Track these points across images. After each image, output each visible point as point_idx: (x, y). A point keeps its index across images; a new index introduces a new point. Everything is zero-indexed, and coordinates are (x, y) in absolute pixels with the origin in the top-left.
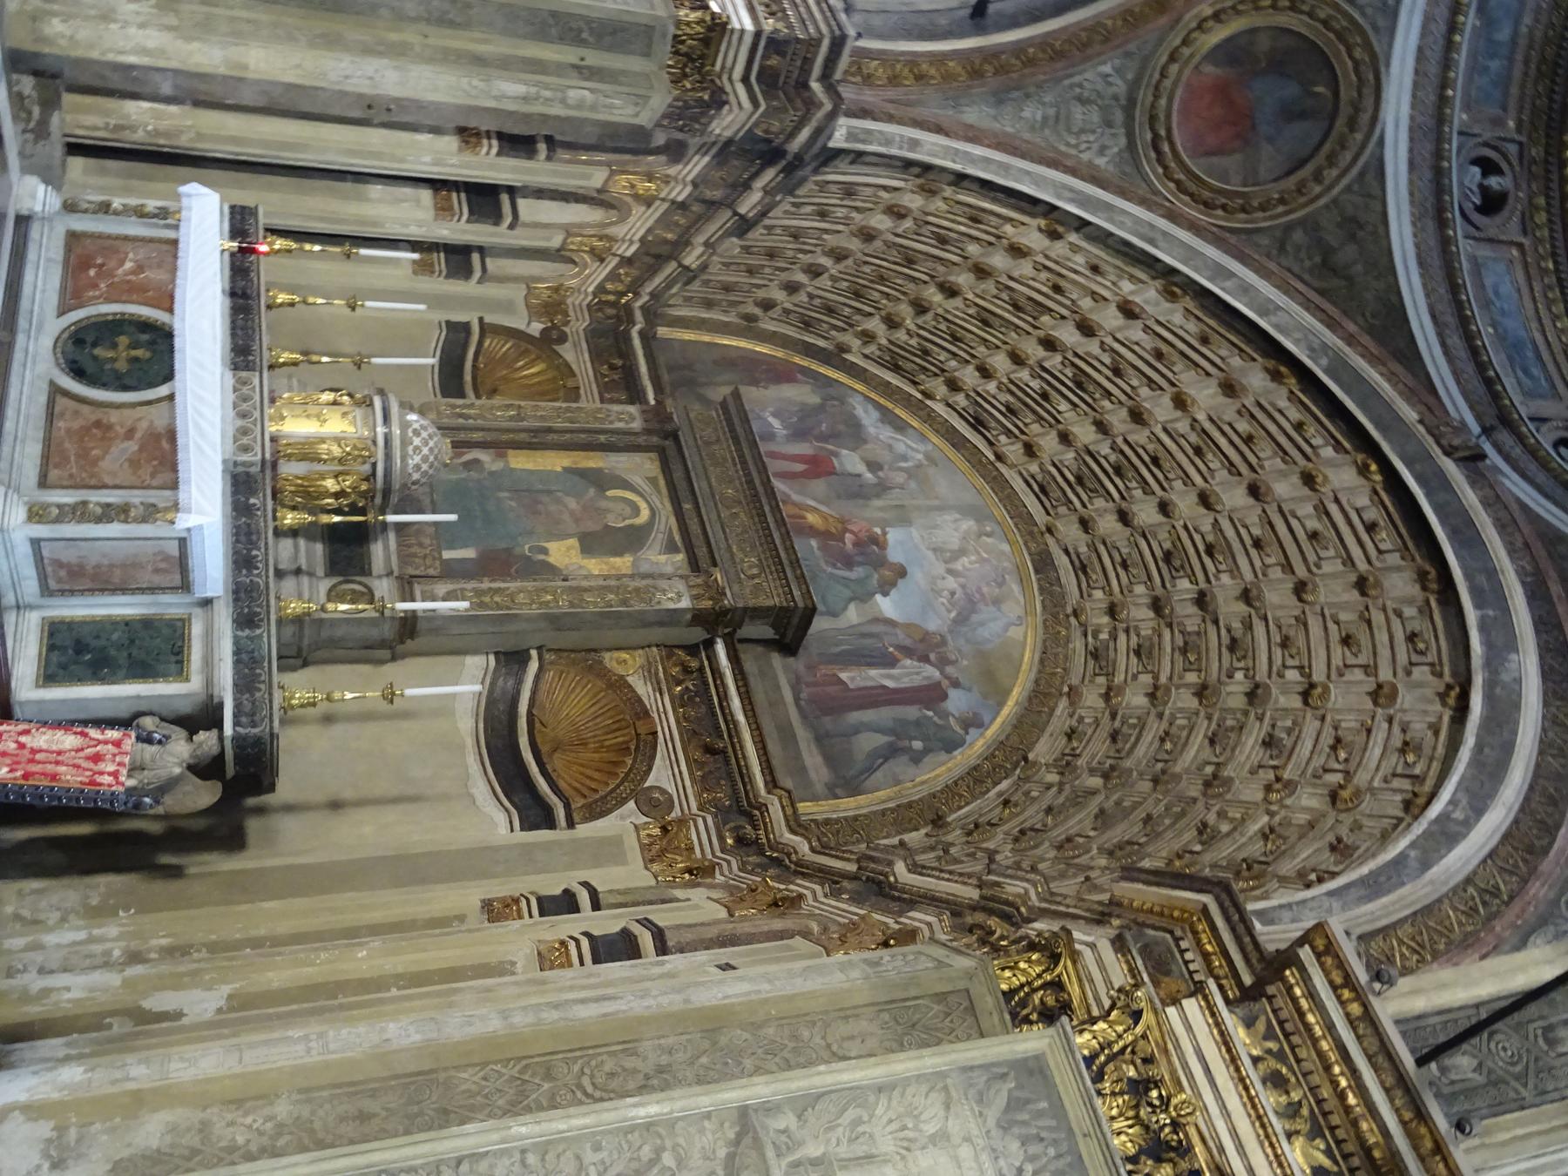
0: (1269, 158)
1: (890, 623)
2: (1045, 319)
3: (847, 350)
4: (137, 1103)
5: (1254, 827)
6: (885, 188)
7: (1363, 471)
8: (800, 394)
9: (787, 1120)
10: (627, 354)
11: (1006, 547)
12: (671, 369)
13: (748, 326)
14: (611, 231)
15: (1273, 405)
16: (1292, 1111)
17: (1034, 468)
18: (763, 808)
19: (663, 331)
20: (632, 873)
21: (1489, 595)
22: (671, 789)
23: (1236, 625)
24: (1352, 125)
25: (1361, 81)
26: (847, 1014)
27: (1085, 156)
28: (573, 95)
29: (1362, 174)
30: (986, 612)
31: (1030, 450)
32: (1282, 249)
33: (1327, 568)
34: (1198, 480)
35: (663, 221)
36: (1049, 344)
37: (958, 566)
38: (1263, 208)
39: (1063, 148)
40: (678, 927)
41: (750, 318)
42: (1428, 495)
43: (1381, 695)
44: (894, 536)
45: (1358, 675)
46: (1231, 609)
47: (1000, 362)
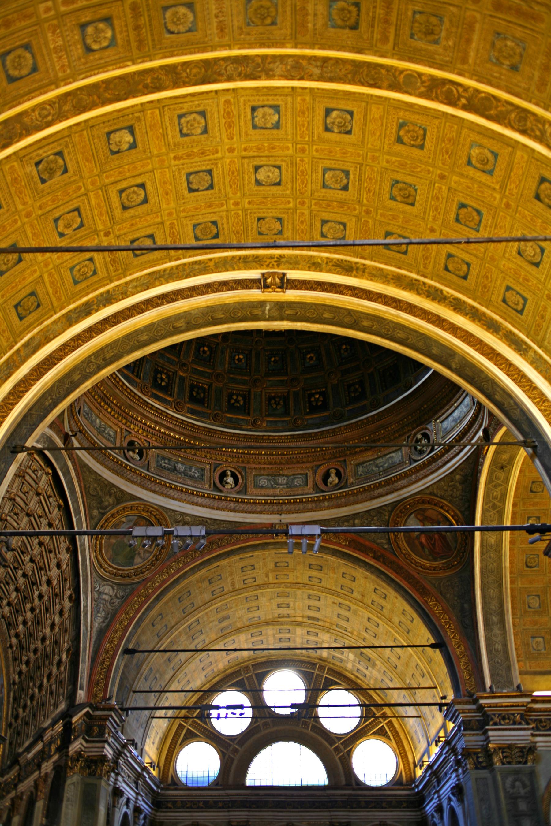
43: (59, 566)
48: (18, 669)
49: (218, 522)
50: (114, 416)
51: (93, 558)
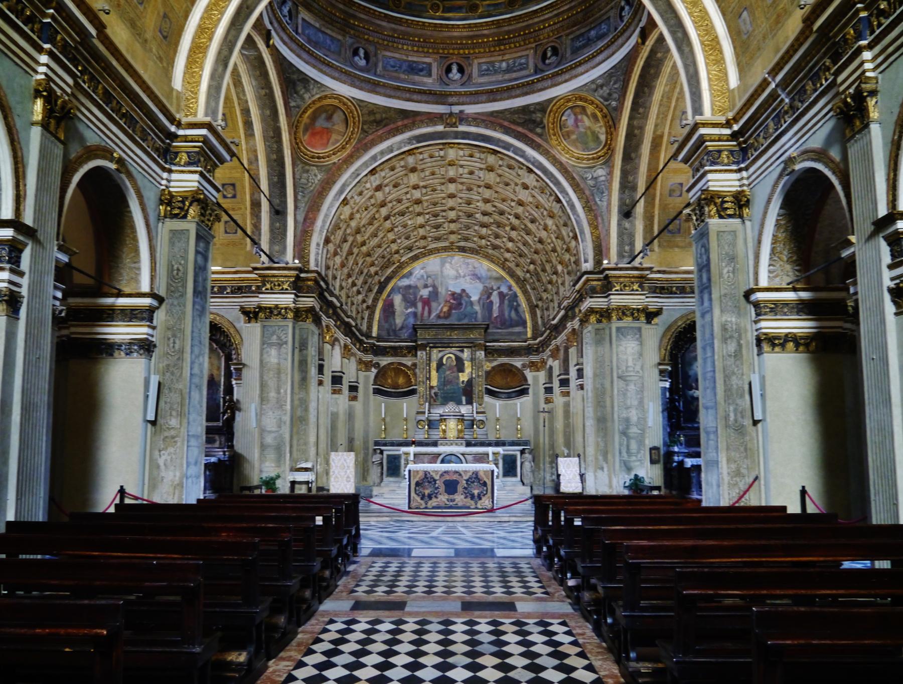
0: (340, 127)
1: (480, 299)
2: (377, 216)
3: (380, 280)
4: (596, 459)
5: (554, 239)
6: (327, 254)
7: (452, 148)
8: (398, 300)
9: (620, 371)
10: (385, 348)
11: (456, 258)
12: (389, 336)
13: (372, 309)
14: (342, 345)
15: (421, 160)
16: (629, 286)
17: (430, 239)
18: (529, 345)
19: (374, 334)
20: (542, 375)
21: (508, 146)
22: (522, 363)
23: (494, 209)
24: (344, 104)
25: (335, 98)
26: (596, 352)
27: (316, 182)
28: (313, 353)
29: (359, 106)
30: (477, 272)
31: (424, 238)
32: (366, 132)
33: (481, 175)
34: (443, 195)
35: (338, 328)
36: (387, 218)
37: (462, 274)
38: (352, 134)
39: (312, 188)
40: (560, 370)
41: (368, 307)
42: (469, 139)
43: (526, 187)
45: (518, 189)
46: (489, 208)
47: (391, 236)
48: (525, 270)
49: (618, 66)
50: (520, 46)
51: (563, 159)
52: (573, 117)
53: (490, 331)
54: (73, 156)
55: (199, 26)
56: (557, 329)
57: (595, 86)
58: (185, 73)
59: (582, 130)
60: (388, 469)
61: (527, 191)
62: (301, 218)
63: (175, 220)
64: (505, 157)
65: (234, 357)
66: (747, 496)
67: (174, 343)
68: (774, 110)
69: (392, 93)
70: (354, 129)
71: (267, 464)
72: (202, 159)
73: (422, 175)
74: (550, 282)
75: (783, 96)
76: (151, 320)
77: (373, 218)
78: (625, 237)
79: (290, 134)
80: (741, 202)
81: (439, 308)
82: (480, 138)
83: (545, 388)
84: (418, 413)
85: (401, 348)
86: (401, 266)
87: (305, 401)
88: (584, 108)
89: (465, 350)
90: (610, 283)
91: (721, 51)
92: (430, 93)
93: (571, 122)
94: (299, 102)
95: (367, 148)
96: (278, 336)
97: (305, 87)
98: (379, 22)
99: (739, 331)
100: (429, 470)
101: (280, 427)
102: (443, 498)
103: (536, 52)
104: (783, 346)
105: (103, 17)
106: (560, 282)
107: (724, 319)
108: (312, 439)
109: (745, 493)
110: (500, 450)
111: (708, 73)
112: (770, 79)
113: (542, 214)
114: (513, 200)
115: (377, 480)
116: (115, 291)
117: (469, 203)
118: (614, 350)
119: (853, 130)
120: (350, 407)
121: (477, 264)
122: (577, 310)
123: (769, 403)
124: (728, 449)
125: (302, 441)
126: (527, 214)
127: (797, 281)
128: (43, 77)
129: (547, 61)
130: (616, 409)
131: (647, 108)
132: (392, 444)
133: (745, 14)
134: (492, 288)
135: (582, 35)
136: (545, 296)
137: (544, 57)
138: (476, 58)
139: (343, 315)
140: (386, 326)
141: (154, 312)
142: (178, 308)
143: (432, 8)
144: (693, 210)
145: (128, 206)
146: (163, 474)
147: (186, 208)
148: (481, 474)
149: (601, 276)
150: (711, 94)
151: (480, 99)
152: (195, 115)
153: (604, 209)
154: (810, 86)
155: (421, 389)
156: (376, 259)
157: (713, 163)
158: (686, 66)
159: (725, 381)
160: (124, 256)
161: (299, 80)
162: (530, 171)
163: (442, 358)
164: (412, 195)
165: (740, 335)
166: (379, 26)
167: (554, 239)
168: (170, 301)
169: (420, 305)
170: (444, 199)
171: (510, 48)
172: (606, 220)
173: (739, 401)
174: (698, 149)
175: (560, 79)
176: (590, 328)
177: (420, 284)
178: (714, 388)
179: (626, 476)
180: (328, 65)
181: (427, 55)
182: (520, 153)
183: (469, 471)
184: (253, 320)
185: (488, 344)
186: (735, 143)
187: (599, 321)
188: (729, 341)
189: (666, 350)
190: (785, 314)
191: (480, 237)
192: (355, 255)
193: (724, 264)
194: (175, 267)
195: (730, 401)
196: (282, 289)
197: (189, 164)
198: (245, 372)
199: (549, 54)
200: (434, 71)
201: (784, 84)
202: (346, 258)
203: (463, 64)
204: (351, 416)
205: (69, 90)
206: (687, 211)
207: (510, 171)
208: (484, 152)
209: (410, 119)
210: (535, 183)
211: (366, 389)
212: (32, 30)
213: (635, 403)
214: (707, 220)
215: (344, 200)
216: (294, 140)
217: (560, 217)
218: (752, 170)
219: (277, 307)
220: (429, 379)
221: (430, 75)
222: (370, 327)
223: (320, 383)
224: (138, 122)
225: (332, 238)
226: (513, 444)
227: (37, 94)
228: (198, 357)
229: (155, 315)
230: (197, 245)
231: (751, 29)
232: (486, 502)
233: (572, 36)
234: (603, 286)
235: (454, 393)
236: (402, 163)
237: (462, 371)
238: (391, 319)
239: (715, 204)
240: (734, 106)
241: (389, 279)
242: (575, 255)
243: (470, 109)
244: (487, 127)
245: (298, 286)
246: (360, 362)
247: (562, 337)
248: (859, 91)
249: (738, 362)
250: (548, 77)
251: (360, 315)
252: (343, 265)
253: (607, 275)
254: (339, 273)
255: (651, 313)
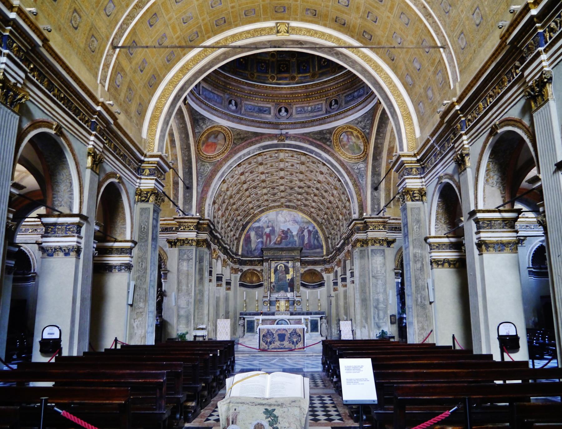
0: (222, 142)
1: (297, 234)
2: (241, 189)
4: (362, 322)
5: (337, 201)
7: (282, 152)
8: (253, 234)
9: (373, 273)
10: (246, 261)
11: (285, 211)
13: (238, 239)
14: (222, 259)
16: (378, 227)
19: (240, 253)
20: (332, 276)
21: (312, 152)
23: (305, 185)
24: (224, 130)
25: (219, 127)
26: (361, 263)
27: (209, 171)
28: (207, 264)
29: (232, 131)
30: (296, 219)
31: (267, 200)
33: (298, 167)
35: (220, 250)
36: (246, 190)
37: (288, 220)
38: (228, 145)
41: (236, 239)
43: (322, 173)
44: (282, 228)
45: (317, 174)
46: (302, 184)
47: (249, 200)
50: (318, 98)
51: (342, 158)
52: (346, 137)
53: (303, 251)
54: (101, 179)
55: (155, 106)
56: (340, 250)
57: (357, 122)
58: (148, 130)
59: (352, 144)
60: (248, 328)
61: (323, 175)
62: (200, 191)
63: (142, 203)
64: (311, 157)
65: (163, 266)
66: (427, 340)
67: (142, 265)
68: (434, 152)
69: (250, 123)
70: (229, 143)
71: (181, 326)
72: (156, 172)
73: (266, 167)
74: (336, 224)
75: (437, 147)
76: (131, 253)
77: (239, 190)
78: (375, 201)
79: (195, 146)
80: (422, 193)
81: (275, 238)
82: (297, 147)
83: (333, 283)
84: (264, 297)
85: (255, 261)
86: (255, 216)
87: (202, 291)
88: (352, 133)
89: (290, 262)
90: (367, 225)
91: (412, 120)
92: (270, 123)
93: (345, 139)
94: (200, 130)
95: (236, 152)
96: (187, 255)
97: (203, 122)
98: (243, 86)
99: (422, 257)
100: (270, 328)
101: (188, 305)
102: (277, 343)
103: (326, 102)
104: (443, 265)
105: (116, 115)
106: (341, 224)
107: (415, 251)
108: (206, 312)
109: (426, 338)
110: (309, 317)
111: (406, 130)
112: (430, 139)
113: (331, 187)
114: (315, 180)
115: (242, 335)
116: (113, 240)
117: (291, 182)
118: (370, 262)
119: (461, 169)
120: (227, 294)
121: (296, 215)
122: (350, 241)
123: (436, 293)
124: (417, 316)
125: (200, 313)
126: (323, 188)
127: (449, 233)
128: (91, 147)
129: (332, 107)
130: (371, 294)
131: (385, 134)
132: (250, 314)
133: (421, 104)
134: (304, 228)
135: (350, 94)
136: (333, 232)
137: (331, 105)
138: (295, 104)
139: (222, 243)
140: (246, 249)
141: (132, 249)
142: (144, 247)
143: (271, 78)
144: (400, 196)
145: (121, 198)
146: (136, 331)
147: (148, 197)
148: (298, 331)
149: (363, 221)
150: (407, 140)
151: (297, 126)
152: (153, 151)
153: (364, 185)
154: (446, 145)
155: (265, 284)
156: (241, 212)
157: (409, 174)
158: (396, 125)
159: (416, 282)
160: (118, 222)
161: (200, 119)
162: (324, 165)
163: (277, 266)
164: (260, 177)
165: (423, 259)
166: (243, 88)
167: (337, 201)
168: (140, 243)
169: (265, 237)
170: (278, 179)
171: (313, 99)
172: (365, 191)
173: (423, 292)
174: (401, 167)
175: (339, 117)
176: (357, 250)
177: (265, 226)
178: (411, 285)
179: (378, 331)
180: (216, 110)
181: (268, 103)
182: (318, 155)
183: (291, 329)
184: (174, 246)
185: (302, 258)
186: (419, 164)
187: (362, 246)
188: (417, 262)
189: (398, 261)
190: (444, 249)
191: (297, 200)
192: (229, 210)
193: (414, 224)
194: (143, 227)
195: (419, 292)
196: (190, 229)
197: (150, 175)
198: (169, 275)
199: (333, 104)
200: (272, 111)
201: (437, 141)
202: (225, 212)
203: (287, 108)
204: (227, 299)
205: (101, 150)
206: (398, 196)
207: (314, 165)
208: (299, 155)
209: (259, 137)
210: (327, 171)
211: (235, 283)
212: (88, 126)
213: (382, 291)
214: (406, 202)
215: (223, 180)
216: (197, 150)
217: (340, 189)
218: (426, 178)
219: (187, 239)
220: (270, 278)
221: (270, 114)
222: (237, 249)
223: (210, 281)
224: (127, 157)
225: (217, 201)
226: (316, 313)
227: (89, 154)
228: (153, 271)
229: (133, 251)
230: (153, 215)
231: (424, 111)
232: (300, 345)
233: (345, 95)
234: (364, 227)
235: (284, 286)
236: (255, 160)
237: (288, 273)
238: (249, 245)
239: (410, 194)
240: (418, 146)
241: (248, 223)
242: (349, 210)
243: (292, 132)
244: (300, 141)
245: (198, 228)
246: (232, 269)
247: (342, 255)
248: (461, 155)
249: (422, 273)
250: (332, 116)
251: (232, 243)
252: (223, 216)
253: (366, 221)
254: (221, 220)
255: (390, 241)
